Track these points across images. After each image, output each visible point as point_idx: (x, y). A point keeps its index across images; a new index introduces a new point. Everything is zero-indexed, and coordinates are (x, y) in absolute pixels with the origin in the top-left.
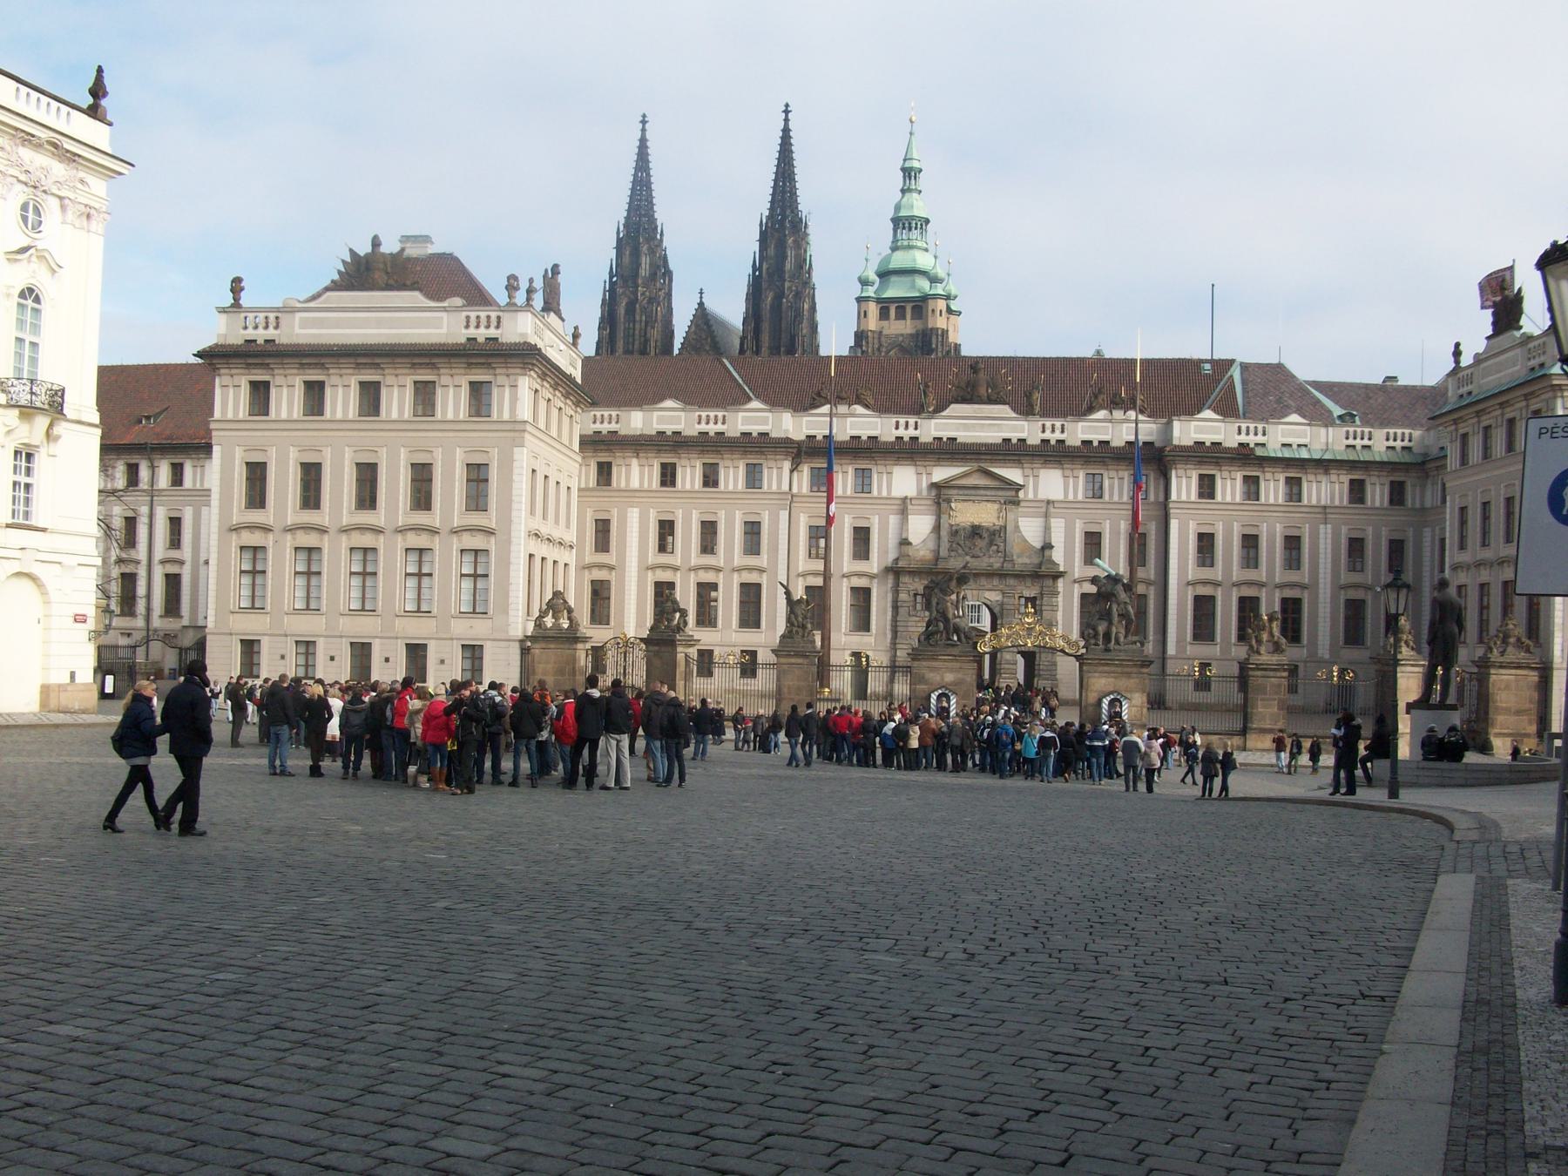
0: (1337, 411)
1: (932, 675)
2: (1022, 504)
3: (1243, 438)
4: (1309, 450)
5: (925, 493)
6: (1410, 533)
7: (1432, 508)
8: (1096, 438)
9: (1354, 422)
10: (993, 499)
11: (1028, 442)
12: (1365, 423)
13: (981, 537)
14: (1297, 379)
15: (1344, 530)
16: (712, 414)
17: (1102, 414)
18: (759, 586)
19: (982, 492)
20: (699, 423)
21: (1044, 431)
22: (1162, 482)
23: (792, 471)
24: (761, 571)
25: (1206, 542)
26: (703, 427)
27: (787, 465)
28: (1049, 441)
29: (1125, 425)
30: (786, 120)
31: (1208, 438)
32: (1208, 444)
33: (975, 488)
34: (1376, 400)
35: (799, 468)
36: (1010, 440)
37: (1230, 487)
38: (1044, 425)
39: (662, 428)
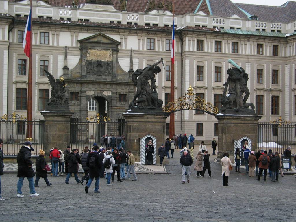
0: (249, 16)
2: (120, 51)
3: (215, 25)
4: (242, 31)
5: (75, 45)
6: (280, 67)
7: (290, 57)
8: (152, 22)
9: (256, 20)
12: (261, 20)
13: (101, 66)
14: (231, 2)
15: (255, 65)
17: (154, 12)
19: (101, 45)
22: (181, 43)
23: (9, 32)
25: (200, 70)
27: (7, 28)
28: (131, 23)
29: (164, 17)
31: (201, 24)
32: (201, 26)
33: (98, 43)
34: (263, 12)
35: (13, 30)
37: (209, 46)
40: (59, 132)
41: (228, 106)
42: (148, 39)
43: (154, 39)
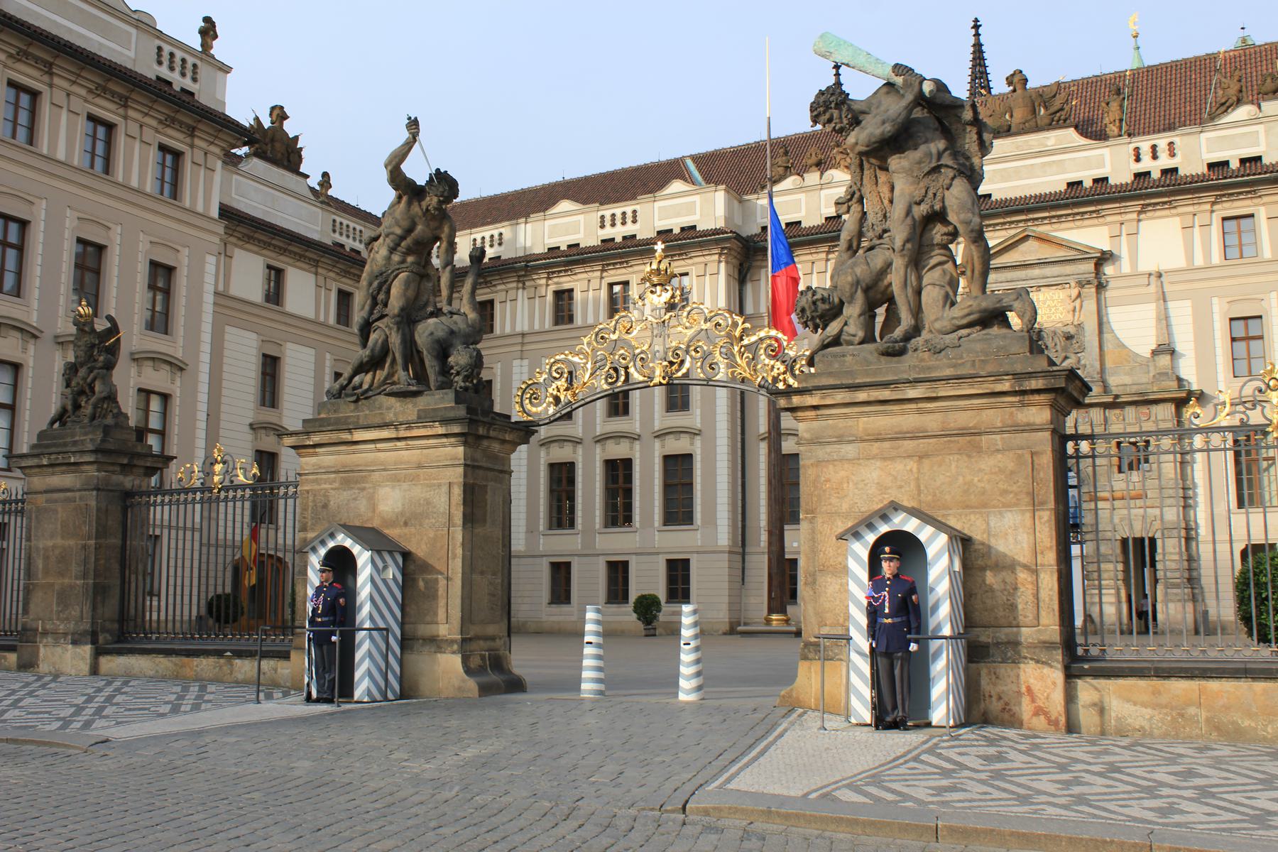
1: (346, 495)
2: (1111, 285)
8: (1233, 155)
10: (1059, 280)
11: (1112, 181)
16: (618, 212)
18: (689, 457)
19: (1036, 272)
20: (602, 227)
21: (1138, 159)
24: (694, 433)
26: (608, 232)
28: (1148, 173)
30: (977, 35)
36: (1080, 183)
38: (1137, 150)
39: (552, 242)
40: (63, 538)
41: (833, 328)
42: (1224, 219)
43: (1252, 216)
